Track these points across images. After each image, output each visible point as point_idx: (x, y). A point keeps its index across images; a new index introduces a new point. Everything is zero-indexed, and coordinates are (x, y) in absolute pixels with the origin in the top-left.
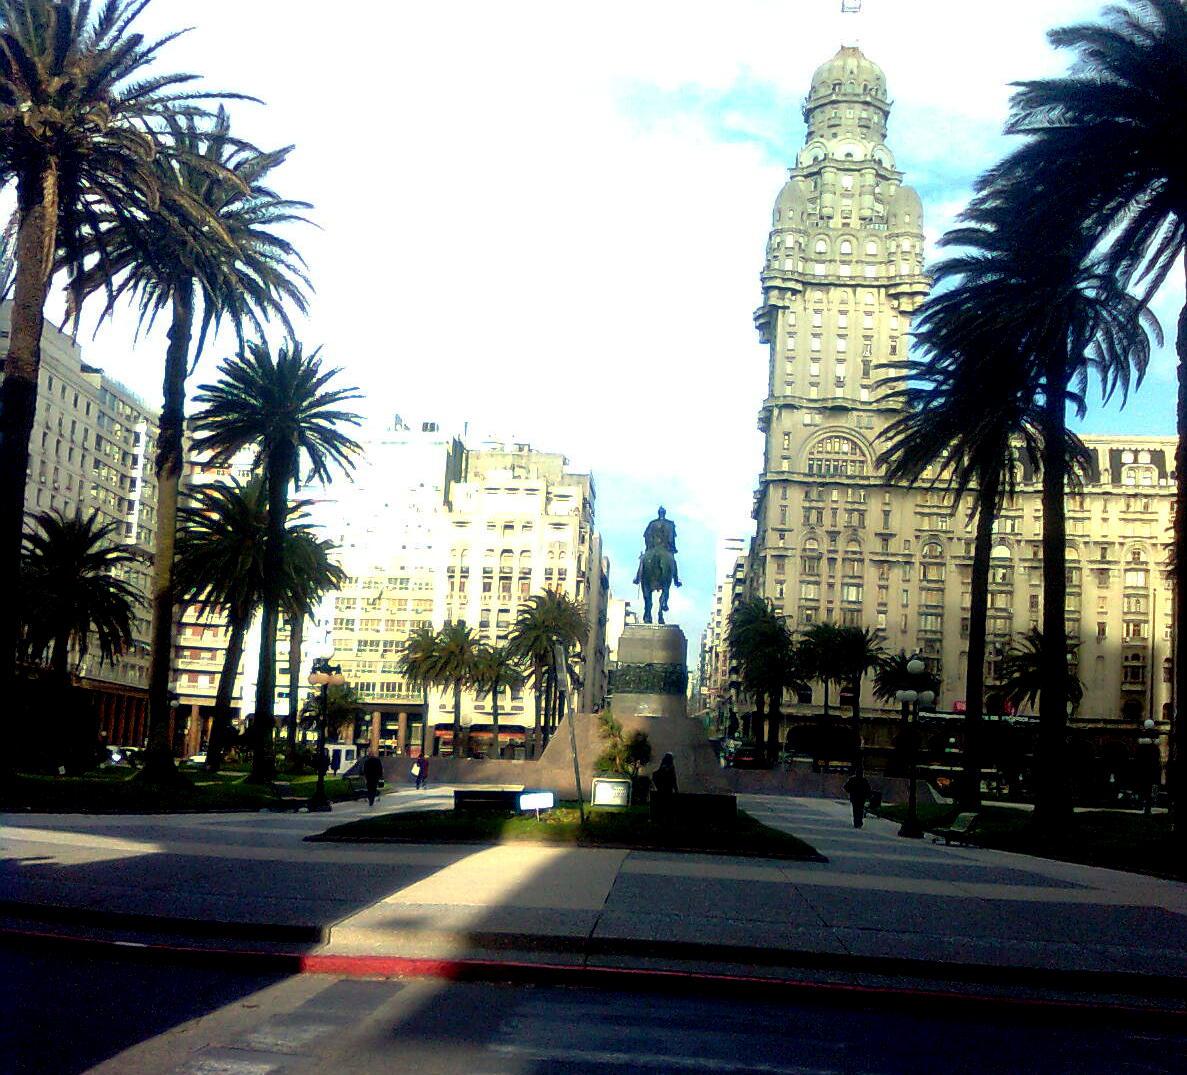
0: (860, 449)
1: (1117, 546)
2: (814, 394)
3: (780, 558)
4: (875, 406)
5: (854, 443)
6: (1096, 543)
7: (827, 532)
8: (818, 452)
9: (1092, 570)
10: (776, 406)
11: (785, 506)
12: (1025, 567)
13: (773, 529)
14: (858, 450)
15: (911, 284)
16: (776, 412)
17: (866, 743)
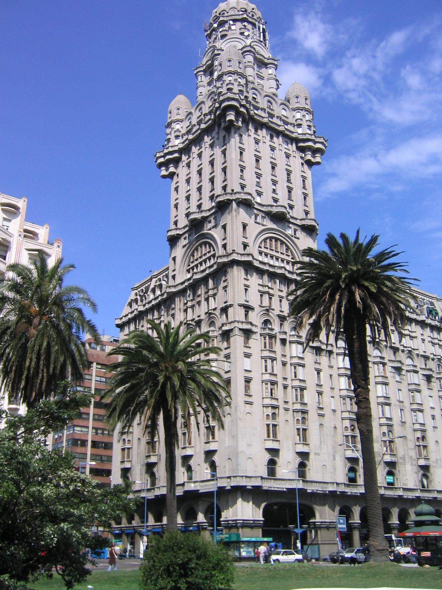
0: (291, 252)
1: (430, 360)
2: (258, 200)
3: (247, 333)
4: (298, 222)
5: (287, 246)
6: (422, 356)
7: (279, 316)
8: (265, 247)
9: (423, 375)
10: (235, 200)
11: (248, 286)
12: (392, 367)
13: (240, 305)
14: (290, 254)
15: (315, 143)
16: (234, 204)
17: (321, 517)
